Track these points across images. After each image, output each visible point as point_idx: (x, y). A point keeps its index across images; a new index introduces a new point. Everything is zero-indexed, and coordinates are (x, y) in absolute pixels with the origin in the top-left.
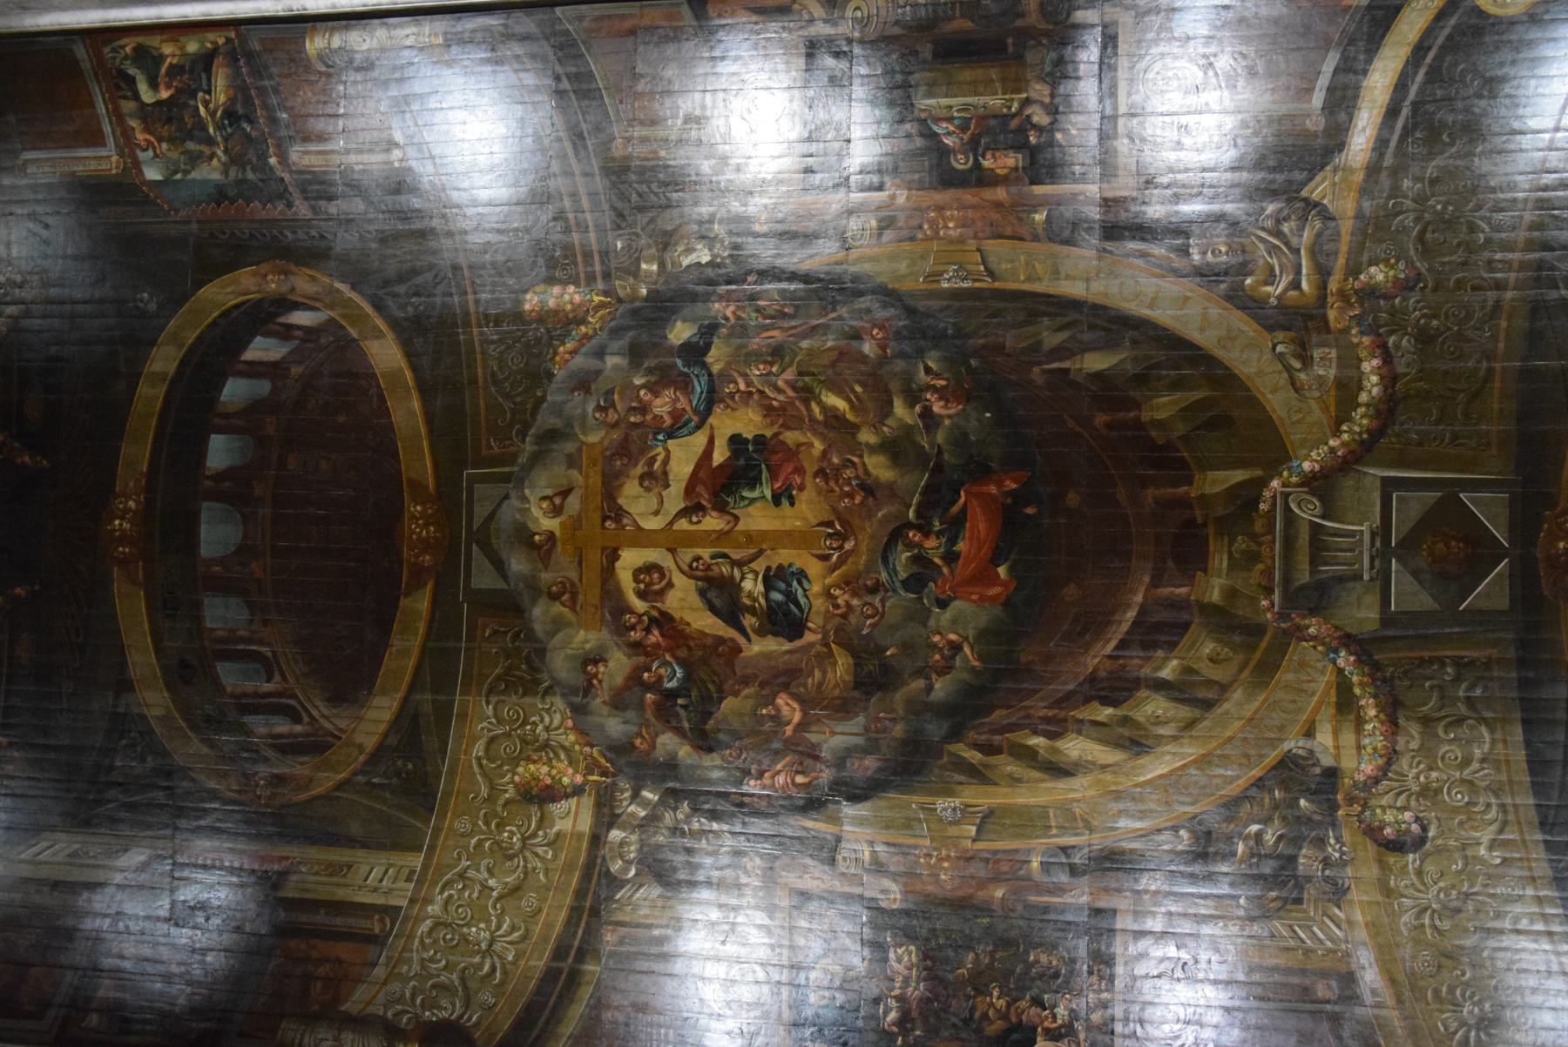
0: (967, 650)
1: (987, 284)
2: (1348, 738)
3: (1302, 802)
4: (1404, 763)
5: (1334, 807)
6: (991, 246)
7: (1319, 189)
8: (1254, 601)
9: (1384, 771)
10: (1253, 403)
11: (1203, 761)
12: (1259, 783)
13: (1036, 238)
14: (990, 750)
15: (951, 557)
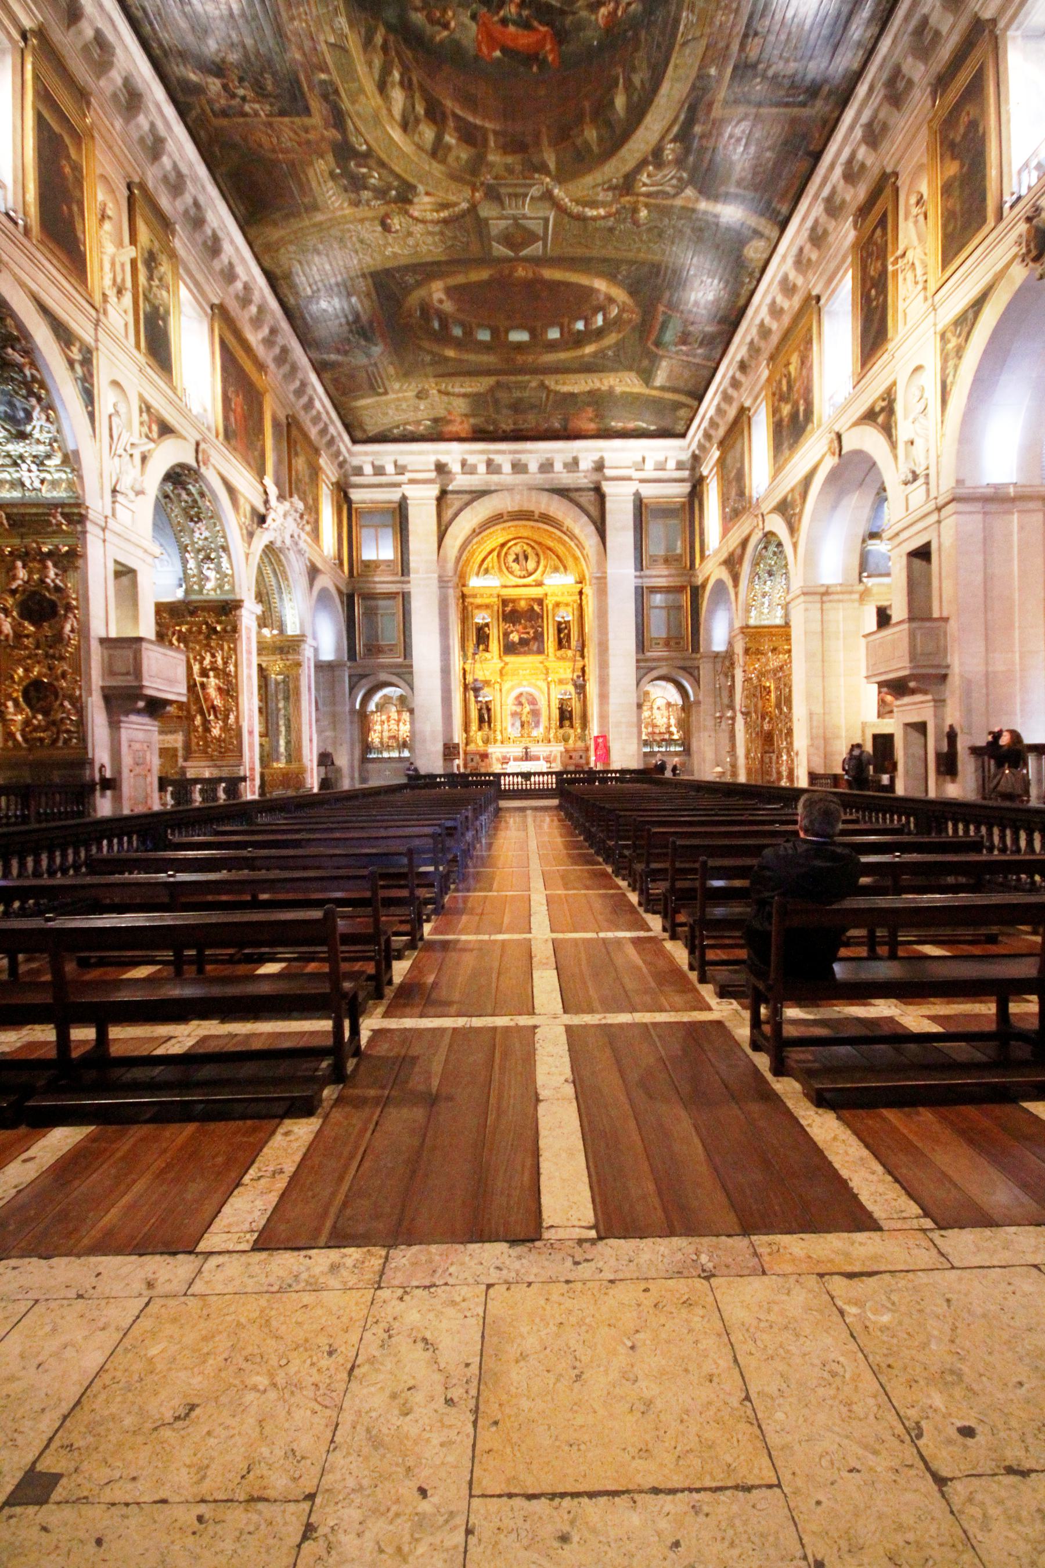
0: (445, 33)
1: (680, 39)
2: (429, 207)
3: (394, 193)
4: (421, 226)
5: (395, 202)
6: (704, 42)
7: (689, 192)
8: (489, 172)
9: (416, 219)
10: (590, 170)
11: (404, 155)
12: (398, 176)
13: (700, 69)
14: (385, 48)
15: (504, 22)
